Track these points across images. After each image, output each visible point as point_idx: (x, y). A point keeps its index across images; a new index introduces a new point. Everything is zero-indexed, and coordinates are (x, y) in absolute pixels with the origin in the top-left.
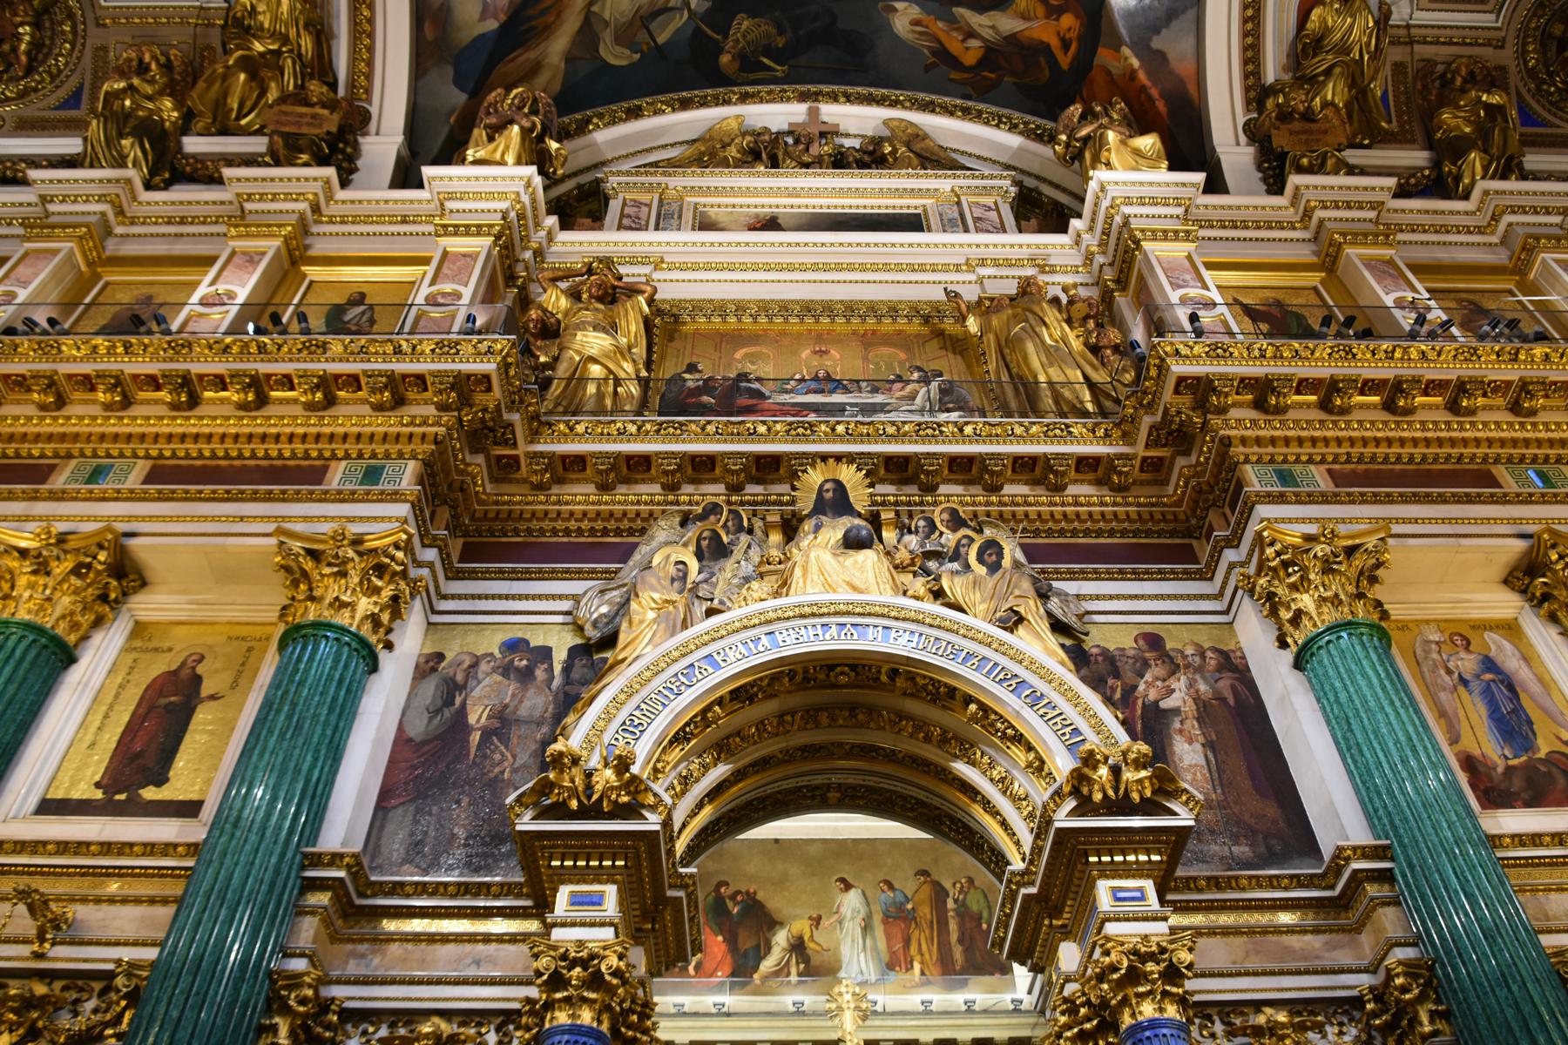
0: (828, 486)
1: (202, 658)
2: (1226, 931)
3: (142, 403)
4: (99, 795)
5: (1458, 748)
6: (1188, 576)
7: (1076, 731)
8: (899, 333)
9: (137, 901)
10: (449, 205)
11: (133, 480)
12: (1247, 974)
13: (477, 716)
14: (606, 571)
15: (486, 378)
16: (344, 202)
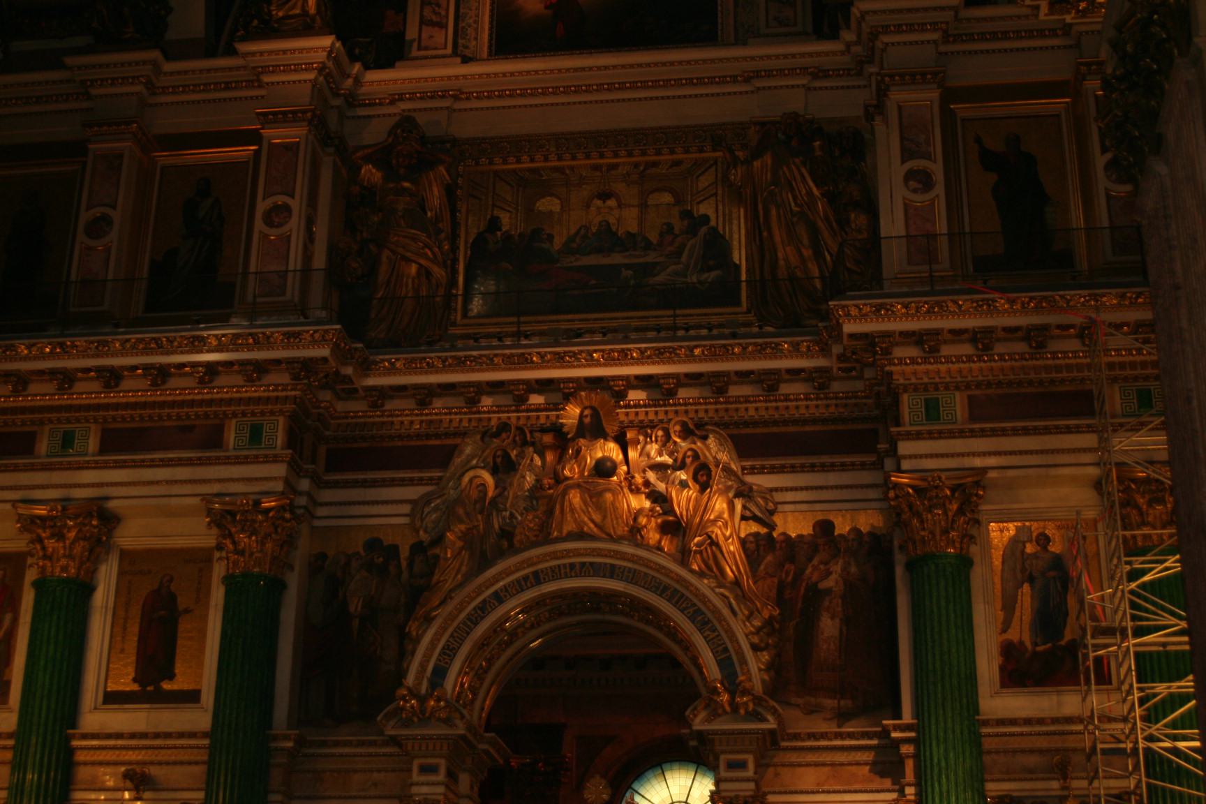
0: (587, 412)
1: (171, 580)
2: (817, 765)
3: (81, 380)
4: (135, 687)
5: (1005, 636)
6: (863, 466)
7: (726, 650)
8: (677, 163)
9: (182, 763)
10: (266, 79)
11: (93, 444)
12: (823, 792)
13: (355, 606)
14: (431, 479)
15: (325, 360)
16: (172, 74)
